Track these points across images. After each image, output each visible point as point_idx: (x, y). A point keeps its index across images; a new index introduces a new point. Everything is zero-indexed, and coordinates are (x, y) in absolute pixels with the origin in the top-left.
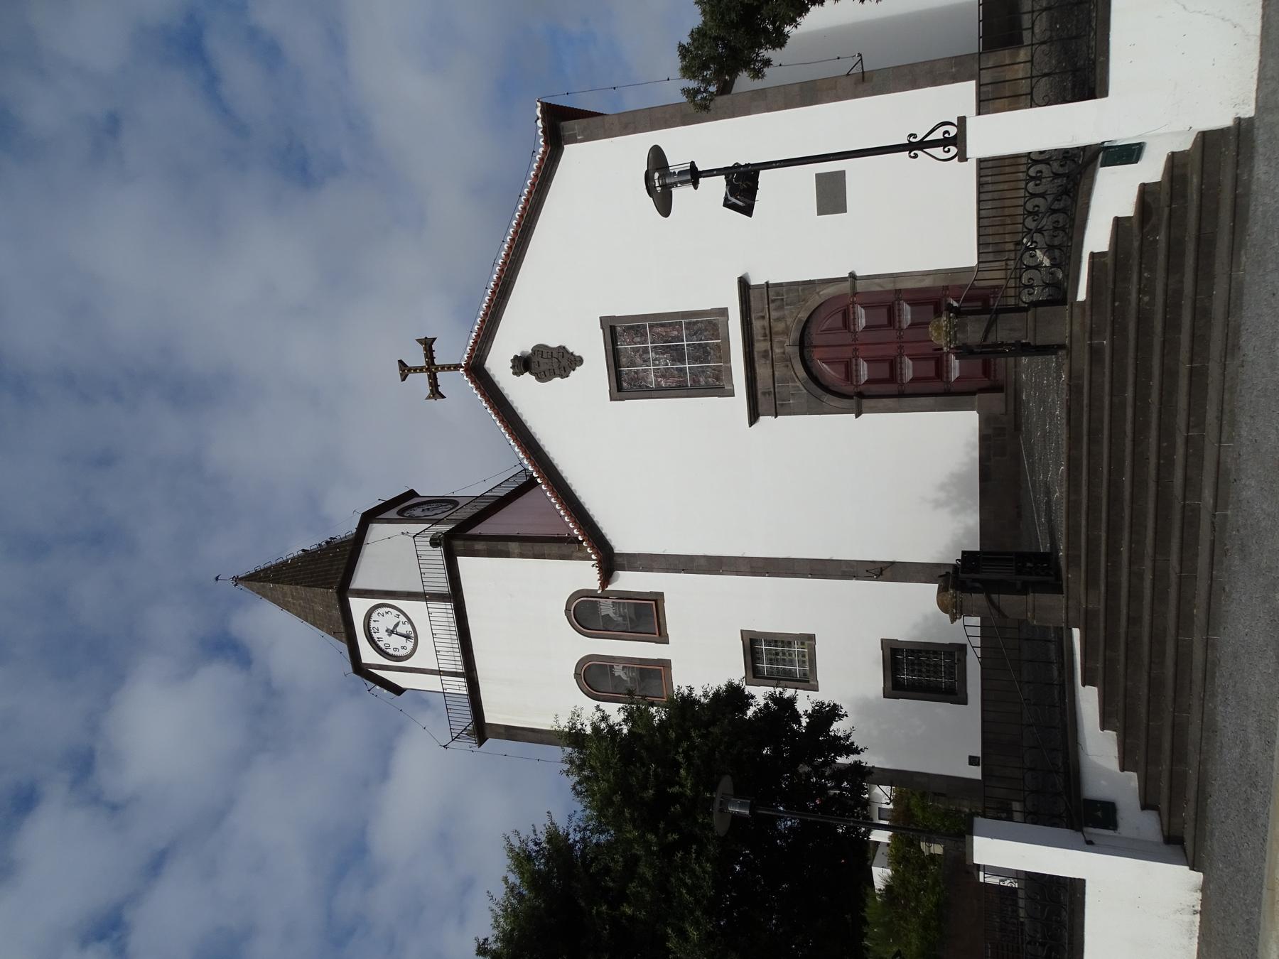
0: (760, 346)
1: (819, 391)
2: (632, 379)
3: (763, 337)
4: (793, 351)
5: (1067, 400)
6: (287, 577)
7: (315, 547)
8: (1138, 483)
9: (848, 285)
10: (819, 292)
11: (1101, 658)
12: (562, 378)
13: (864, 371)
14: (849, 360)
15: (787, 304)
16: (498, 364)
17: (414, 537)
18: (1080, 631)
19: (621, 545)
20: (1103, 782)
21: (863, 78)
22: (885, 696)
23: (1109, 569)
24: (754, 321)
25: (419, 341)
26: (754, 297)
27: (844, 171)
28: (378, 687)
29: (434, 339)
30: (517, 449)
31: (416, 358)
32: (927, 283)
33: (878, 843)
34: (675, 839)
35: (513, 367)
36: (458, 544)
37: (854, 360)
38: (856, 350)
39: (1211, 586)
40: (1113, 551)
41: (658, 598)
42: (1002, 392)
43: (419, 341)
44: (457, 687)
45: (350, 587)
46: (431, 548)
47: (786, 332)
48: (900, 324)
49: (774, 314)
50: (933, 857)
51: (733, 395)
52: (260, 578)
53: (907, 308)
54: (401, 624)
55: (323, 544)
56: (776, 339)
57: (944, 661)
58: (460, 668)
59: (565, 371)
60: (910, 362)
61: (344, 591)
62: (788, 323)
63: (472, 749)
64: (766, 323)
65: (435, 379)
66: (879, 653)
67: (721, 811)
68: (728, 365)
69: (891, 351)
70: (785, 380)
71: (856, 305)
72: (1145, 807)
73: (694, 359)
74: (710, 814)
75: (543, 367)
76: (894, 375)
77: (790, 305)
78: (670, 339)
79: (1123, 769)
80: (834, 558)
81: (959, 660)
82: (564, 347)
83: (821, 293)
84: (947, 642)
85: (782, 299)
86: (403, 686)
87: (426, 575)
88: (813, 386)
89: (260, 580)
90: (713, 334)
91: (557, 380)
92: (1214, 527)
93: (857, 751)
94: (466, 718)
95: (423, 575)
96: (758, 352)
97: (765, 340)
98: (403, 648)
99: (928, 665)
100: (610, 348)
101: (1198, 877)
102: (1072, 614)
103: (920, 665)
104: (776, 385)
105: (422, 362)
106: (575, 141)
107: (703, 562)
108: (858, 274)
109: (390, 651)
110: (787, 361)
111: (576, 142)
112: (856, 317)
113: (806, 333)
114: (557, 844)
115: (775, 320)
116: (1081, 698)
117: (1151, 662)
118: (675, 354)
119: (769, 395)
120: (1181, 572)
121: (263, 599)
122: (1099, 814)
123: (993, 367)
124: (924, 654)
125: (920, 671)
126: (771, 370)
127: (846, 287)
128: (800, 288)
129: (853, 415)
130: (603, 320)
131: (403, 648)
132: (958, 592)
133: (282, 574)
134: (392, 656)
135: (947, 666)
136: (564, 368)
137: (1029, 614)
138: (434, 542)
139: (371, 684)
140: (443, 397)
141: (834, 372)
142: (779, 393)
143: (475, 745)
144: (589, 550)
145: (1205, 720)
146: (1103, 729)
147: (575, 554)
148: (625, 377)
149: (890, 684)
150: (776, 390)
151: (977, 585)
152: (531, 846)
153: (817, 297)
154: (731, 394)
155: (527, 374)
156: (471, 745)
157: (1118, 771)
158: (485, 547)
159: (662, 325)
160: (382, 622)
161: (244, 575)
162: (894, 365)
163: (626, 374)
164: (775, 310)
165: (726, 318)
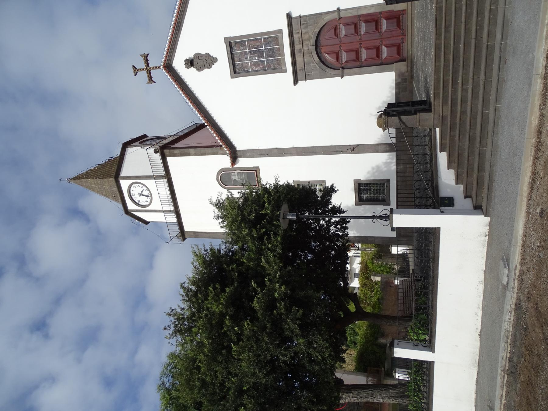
0: (297, 47)
1: (325, 67)
5: (435, 15)
6: (91, 176)
7: (103, 162)
8: (467, 44)
9: (336, 14)
10: (324, 18)
11: (448, 137)
12: (208, 69)
13: (344, 56)
16: (178, 64)
17: (146, 149)
18: (439, 129)
19: (239, 146)
20: (448, 190)
22: (355, 205)
23: (453, 92)
24: (294, 35)
25: (141, 55)
28: (137, 221)
29: (148, 54)
30: (190, 104)
31: (141, 64)
32: (372, 11)
33: (355, 288)
34: (264, 231)
35: (185, 64)
36: (166, 151)
37: (340, 52)
38: (341, 46)
39: (498, 80)
40: (455, 82)
41: (256, 170)
42: (405, 61)
43: (141, 55)
44: (171, 216)
45: (120, 176)
46: (155, 154)
47: (309, 39)
49: (304, 31)
50: (376, 283)
51: (286, 72)
52: (80, 178)
53: (363, 24)
54: (144, 190)
55: (107, 161)
56: (304, 43)
57: (380, 187)
58: (172, 208)
61: (117, 177)
62: (310, 35)
63: (180, 243)
64: (300, 35)
65: (150, 74)
66: (352, 186)
67: (283, 218)
68: (284, 57)
70: (309, 63)
71: (340, 25)
72: (466, 197)
73: (268, 56)
74: (279, 220)
75: (200, 64)
76: (358, 58)
77: (311, 25)
78: (257, 47)
79: (457, 184)
80: (333, 145)
81: (386, 186)
82: (208, 54)
83: (324, 19)
84: (382, 179)
85: (307, 23)
86: (148, 220)
87: (154, 167)
89: (80, 178)
90: (276, 43)
91: (206, 70)
92: (501, 50)
93: (343, 212)
94: (177, 231)
95: (152, 167)
96: (296, 50)
98: (146, 201)
99: (374, 190)
101: (488, 219)
102: (436, 122)
103: (370, 190)
105: (143, 66)
107: (276, 151)
108: (341, 8)
109: (141, 203)
110: (310, 53)
112: (341, 30)
113: (318, 40)
114: (216, 256)
115: (304, 34)
116: (439, 158)
117: (470, 129)
118: (259, 54)
119: (302, 70)
120: (485, 79)
121: (82, 187)
122: (447, 202)
124: (372, 185)
125: (370, 193)
126: (303, 58)
127: (335, 16)
129: (340, 78)
131: (146, 201)
132: (386, 117)
133: (89, 175)
134: (140, 205)
135: (382, 189)
137: (417, 124)
138: (156, 151)
139: (133, 219)
140: (155, 82)
141: (332, 58)
143: (181, 241)
144: (225, 149)
145: (493, 146)
146: (449, 169)
147: (219, 152)
148: (237, 67)
149: (358, 199)
151: (395, 113)
152: (203, 252)
155: (192, 68)
156: (179, 241)
157: (455, 185)
158: (179, 152)
159: (253, 40)
160: (136, 190)
161: (73, 177)
162: (357, 52)
164: (303, 28)
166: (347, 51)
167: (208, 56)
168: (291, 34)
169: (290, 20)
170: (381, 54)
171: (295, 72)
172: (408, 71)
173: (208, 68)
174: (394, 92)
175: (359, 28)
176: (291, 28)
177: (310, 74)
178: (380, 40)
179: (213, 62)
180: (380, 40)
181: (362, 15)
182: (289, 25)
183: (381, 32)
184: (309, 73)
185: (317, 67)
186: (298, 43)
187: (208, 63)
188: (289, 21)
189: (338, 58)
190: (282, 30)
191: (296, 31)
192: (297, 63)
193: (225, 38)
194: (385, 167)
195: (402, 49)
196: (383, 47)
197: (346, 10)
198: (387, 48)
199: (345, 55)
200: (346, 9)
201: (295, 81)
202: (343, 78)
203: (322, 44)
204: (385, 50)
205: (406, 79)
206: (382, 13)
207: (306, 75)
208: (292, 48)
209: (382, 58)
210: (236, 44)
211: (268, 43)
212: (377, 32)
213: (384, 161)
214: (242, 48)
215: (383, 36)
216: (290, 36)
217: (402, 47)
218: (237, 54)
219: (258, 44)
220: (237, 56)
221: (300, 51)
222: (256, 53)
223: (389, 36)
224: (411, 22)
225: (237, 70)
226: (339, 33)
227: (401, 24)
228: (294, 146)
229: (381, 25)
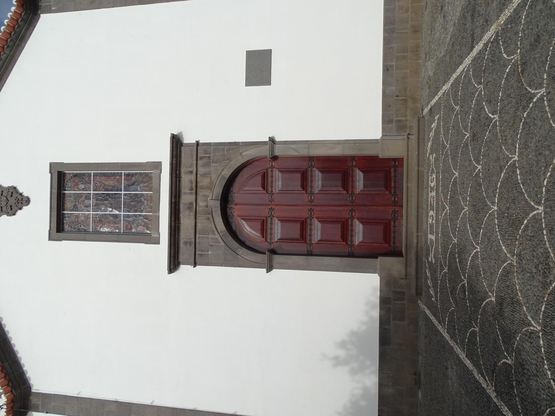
0: (186, 198)
1: (235, 244)
2: (73, 223)
3: (190, 190)
4: (216, 205)
9: (267, 148)
10: (243, 152)
14: (265, 218)
15: (213, 162)
26: (184, 154)
27: (269, 52)
32: (337, 152)
37: (269, 219)
47: (210, 187)
48: (312, 189)
49: (201, 170)
56: (201, 193)
59: (11, 209)
60: (319, 224)
62: (213, 179)
64: (193, 177)
68: (157, 214)
69: (303, 213)
71: (274, 170)
73: (129, 208)
76: (304, 236)
77: (216, 162)
78: (110, 188)
82: (15, 188)
83: (243, 154)
85: (210, 157)
88: (230, 239)
97: (191, 193)
100: (55, 191)
104: (197, 236)
106: (49, 11)
108: (277, 139)
110: (209, 214)
111: (51, 12)
119: (190, 244)
126: (194, 221)
127: (265, 151)
128: (226, 148)
129: (264, 270)
130: (52, 166)
136: (11, 206)
142: (199, 243)
148: (66, 220)
150: (197, 241)
153: (240, 157)
154: (157, 241)
162: (304, 225)
163: (68, 217)
165: (159, 171)
167: (12, 193)
168: (176, 174)
169: (177, 148)
170: (352, 236)
171: (175, 245)
173: (8, 214)
174: (376, 313)
175: (309, 180)
176: (177, 160)
177: (202, 253)
179: (20, 204)
180: (350, 208)
182: (174, 156)
183: (353, 194)
184: (202, 251)
185: (220, 243)
186: (189, 191)
187: (9, 204)
188: (174, 149)
189: (264, 230)
190: (160, 163)
191: (186, 168)
192: (182, 228)
193: (51, 164)
195: (394, 232)
196: (356, 222)
197: (286, 143)
199: (279, 228)
200: (286, 141)
201: (172, 264)
202: (270, 271)
203: (236, 201)
204: (359, 228)
205: (403, 293)
206: (356, 159)
207: (197, 256)
208: (173, 198)
209: (353, 243)
210: (71, 177)
211: (133, 184)
212: (345, 192)
214: (82, 186)
216: (174, 176)
217: (395, 226)
218: (70, 196)
219: (111, 183)
220: (70, 200)
221: (190, 208)
222: (106, 200)
225: (66, 227)
226: (269, 185)
227: (393, 185)
228: (153, 402)
229: (353, 181)
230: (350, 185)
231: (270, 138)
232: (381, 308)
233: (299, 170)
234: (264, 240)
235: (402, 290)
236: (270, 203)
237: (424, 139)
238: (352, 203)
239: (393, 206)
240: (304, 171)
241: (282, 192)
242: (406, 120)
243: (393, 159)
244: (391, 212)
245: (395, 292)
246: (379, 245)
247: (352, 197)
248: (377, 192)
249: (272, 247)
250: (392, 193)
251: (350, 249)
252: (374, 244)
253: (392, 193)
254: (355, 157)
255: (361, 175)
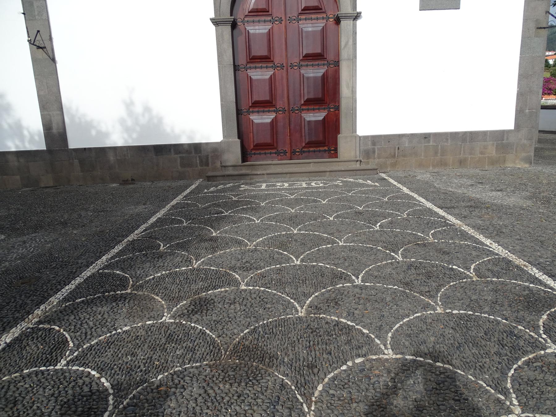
14: (270, 13)
21: (541, 28)
32: (344, 91)
37: (269, 18)
38: (281, 20)
69: (278, 59)
71: (325, 21)
76: (254, 60)
108: (359, 22)
112: (314, 21)
123: (263, 152)
129: (213, 16)
166: (269, 34)
170: (258, 112)
172: (223, 168)
174: (184, 140)
178: (286, 109)
180: (286, 109)
181: (339, 69)
183: (301, 110)
194: (10, 126)
195: (265, 154)
196: (272, 116)
197: (355, 33)
198: (271, 122)
199: (261, 31)
200: (356, 33)
205: (207, 164)
206: (337, 111)
209: (251, 114)
212: (303, 102)
213: (25, 123)
215: (293, 114)
217: (271, 153)
223: (292, 126)
224: (317, 170)
229: (314, 110)
230: (310, 107)
231: (360, 13)
232: (190, 145)
233: (325, 50)
234: (247, 13)
235: (210, 163)
236: (288, 18)
237: (356, 175)
238: (292, 110)
239: (291, 150)
240: (323, 56)
241: (300, 32)
242: (375, 158)
243: (337, 148)
244: (285, 149)
245: (207, 157)
246: (252, 140)
247: (297, 110)
248: (303, 134)
249: (239, 24)
250: (303, 149)
251: (245, 110)
252: (252, 134)
253: (303, 149)
254: (339, 110)
255: (321, 118)
